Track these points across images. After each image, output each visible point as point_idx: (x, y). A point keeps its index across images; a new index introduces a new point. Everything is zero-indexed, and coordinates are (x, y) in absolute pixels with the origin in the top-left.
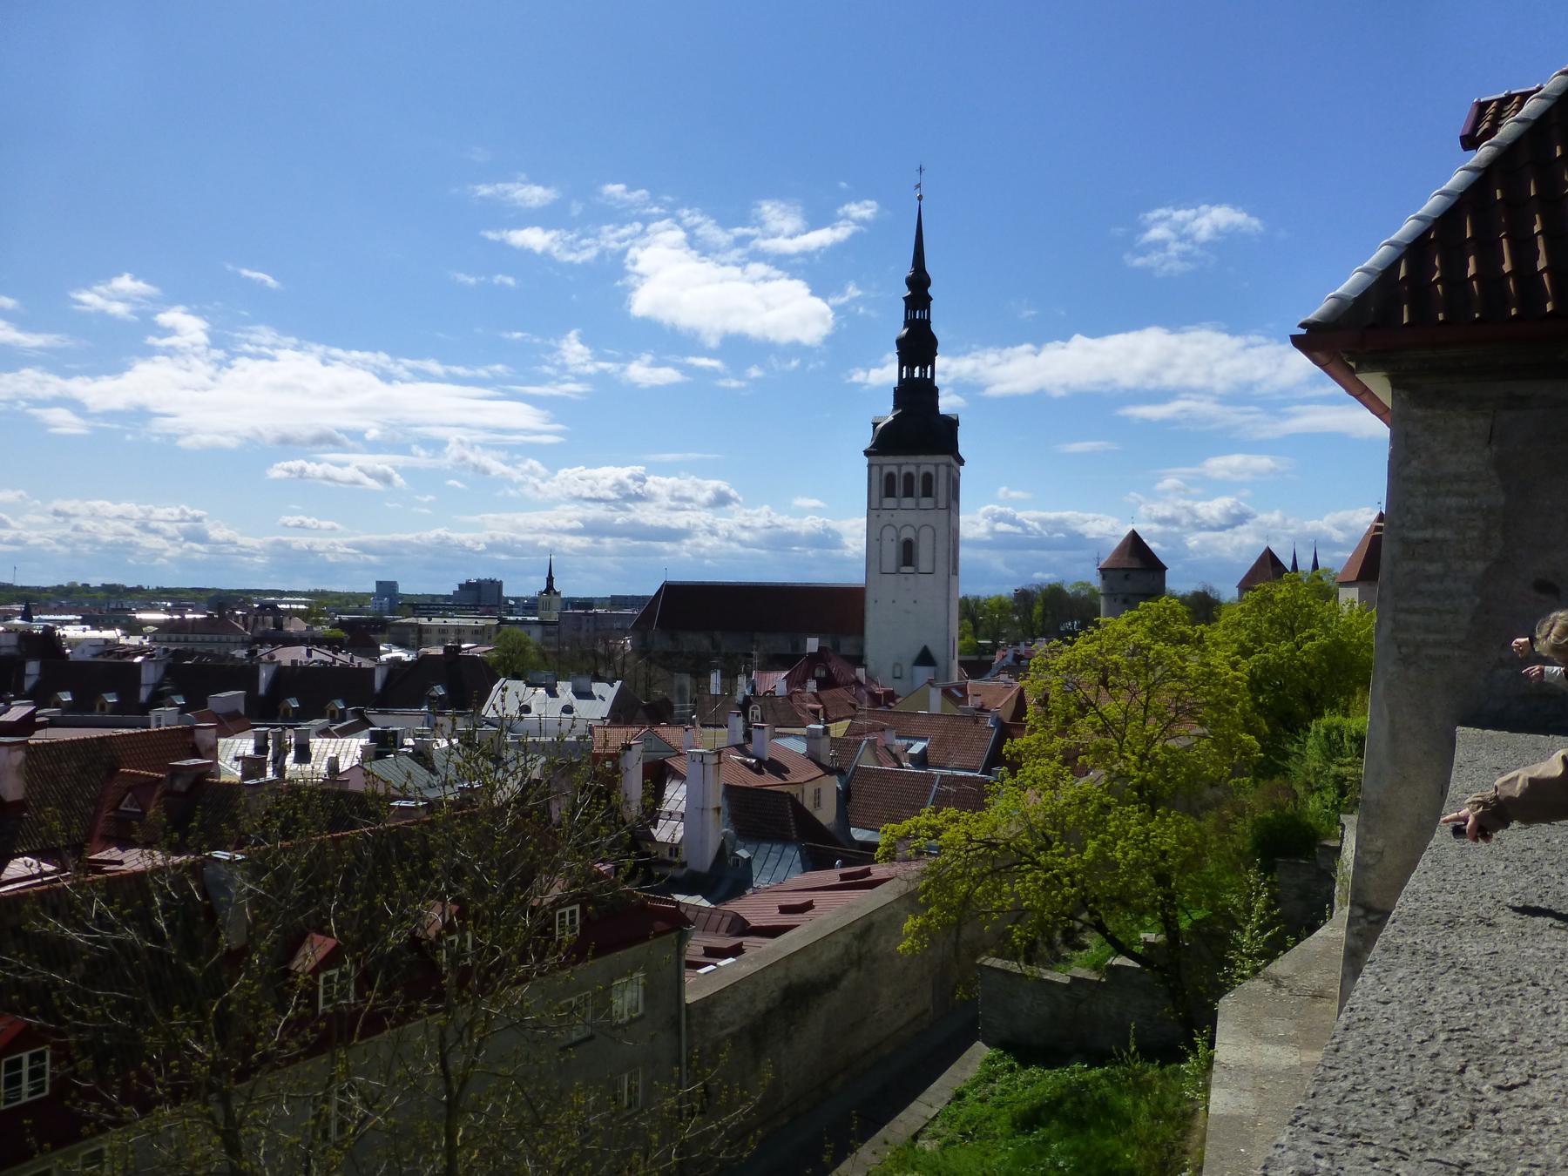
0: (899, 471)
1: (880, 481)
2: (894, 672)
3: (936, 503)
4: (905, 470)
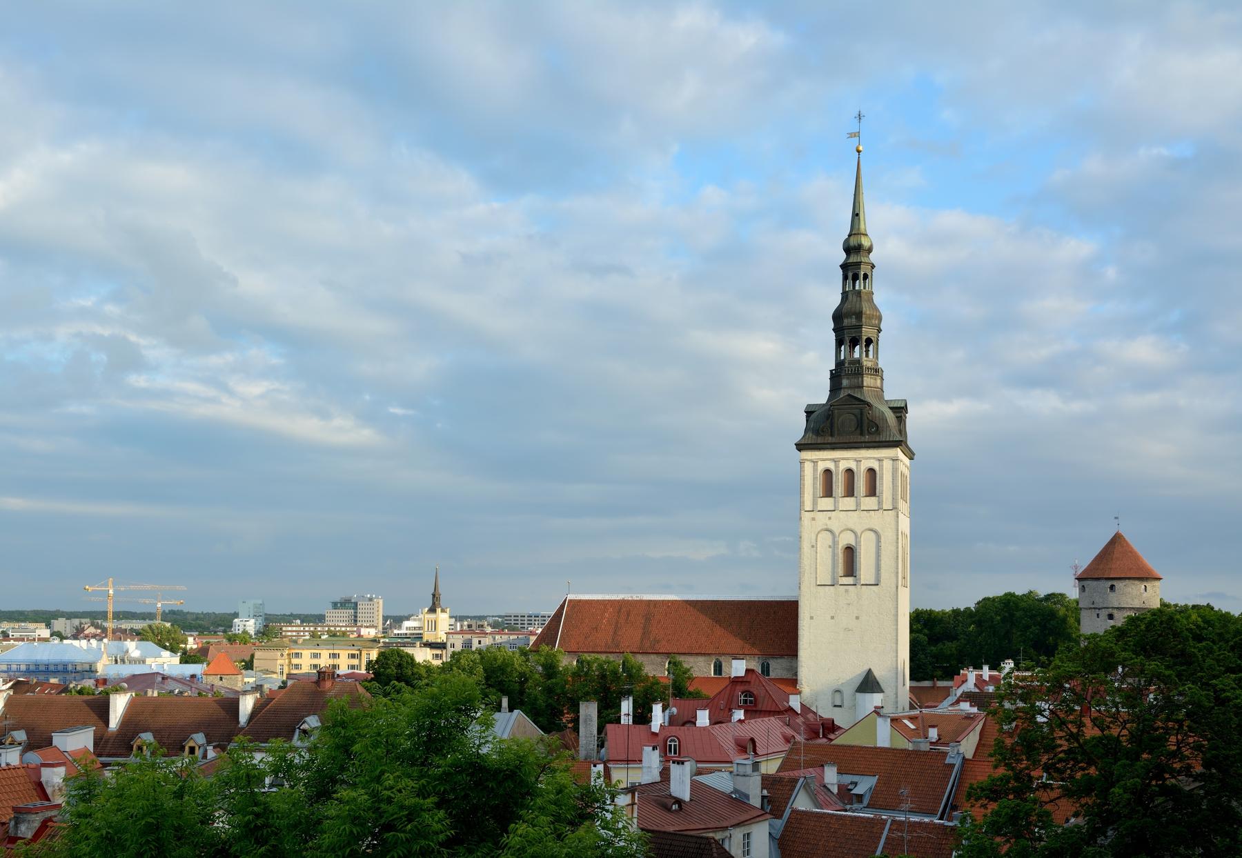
0: (837, 467)
1: (815, 478)
2: (833, 698)
3: (880, 503)
4: (843, 465)
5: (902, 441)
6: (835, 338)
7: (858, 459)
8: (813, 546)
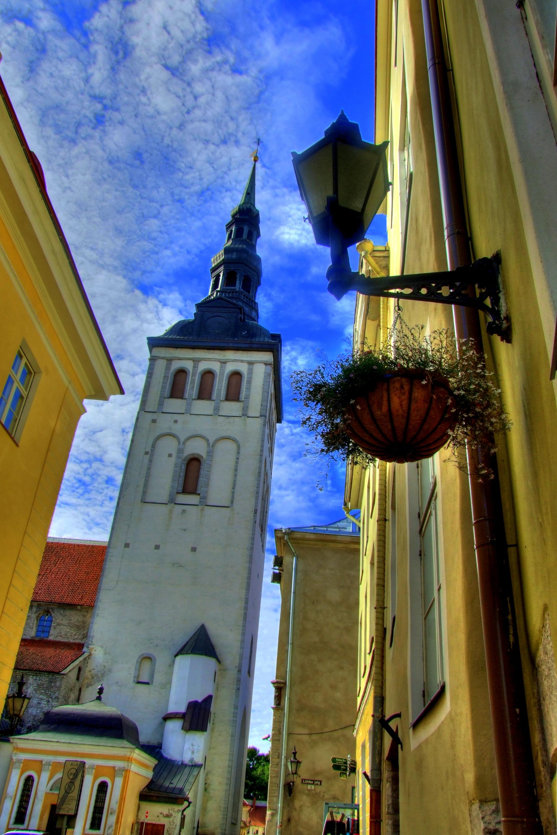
0: (195, 367)
1: (165, 377)
2: (139, 669)
3: (245, 409)
4: (203, 366)
8: (147, 453)
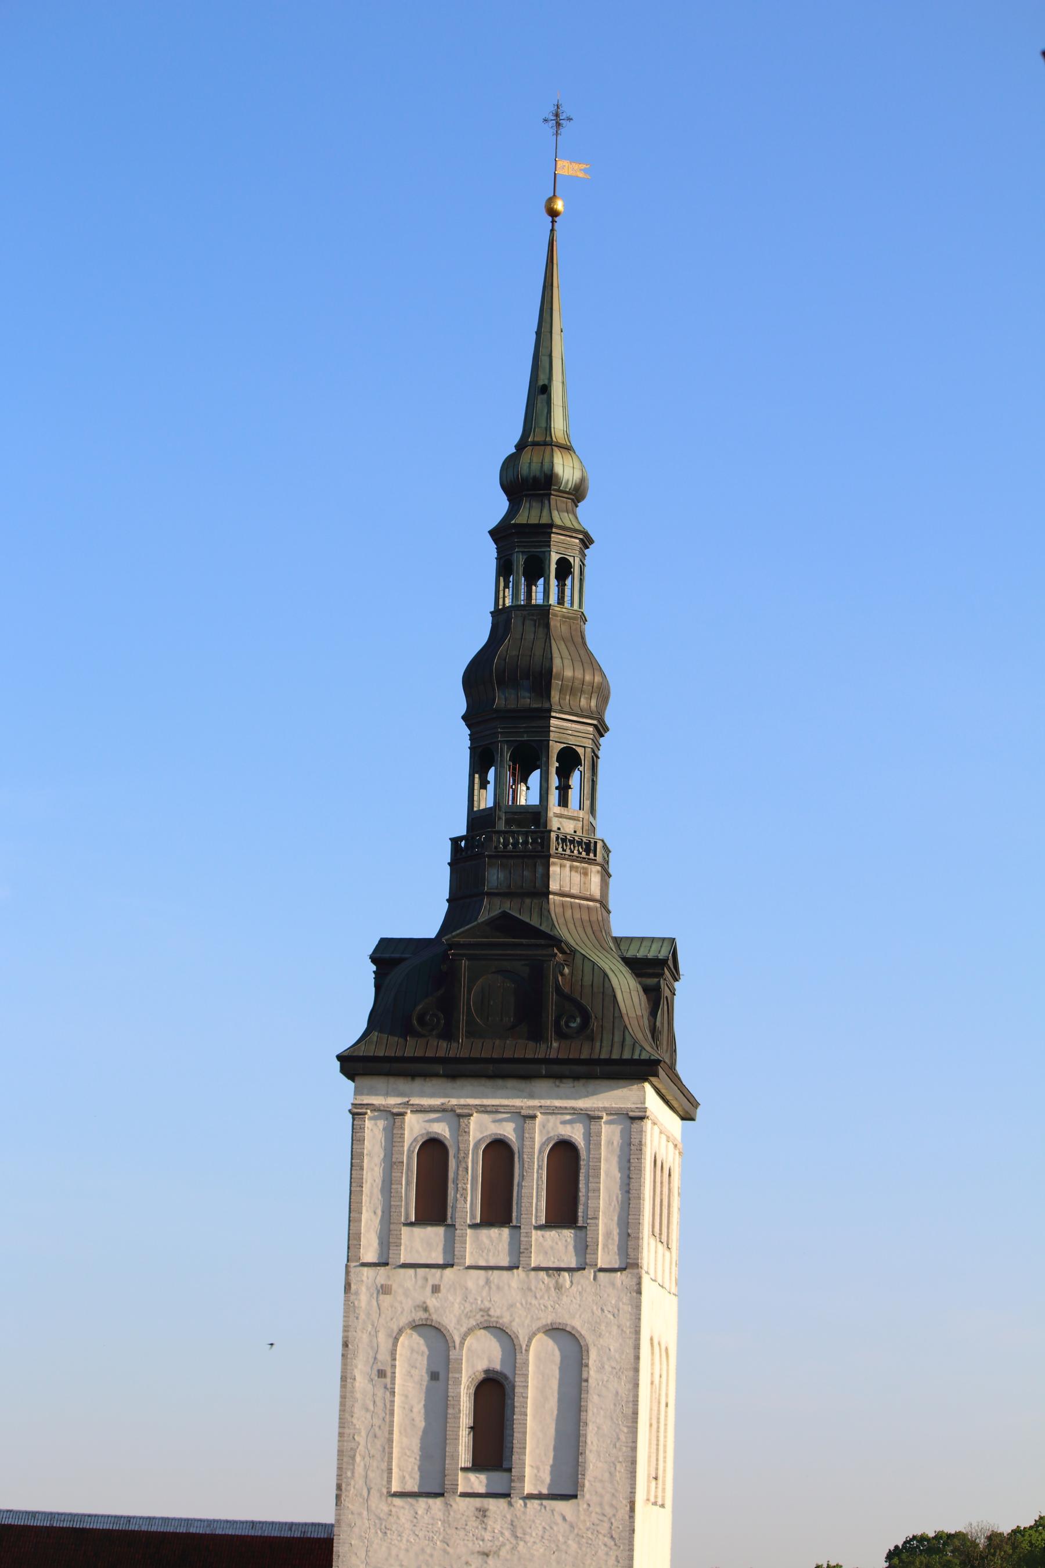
5: (657, 1062)
6: (468, 743)
7: (524, 1112)
